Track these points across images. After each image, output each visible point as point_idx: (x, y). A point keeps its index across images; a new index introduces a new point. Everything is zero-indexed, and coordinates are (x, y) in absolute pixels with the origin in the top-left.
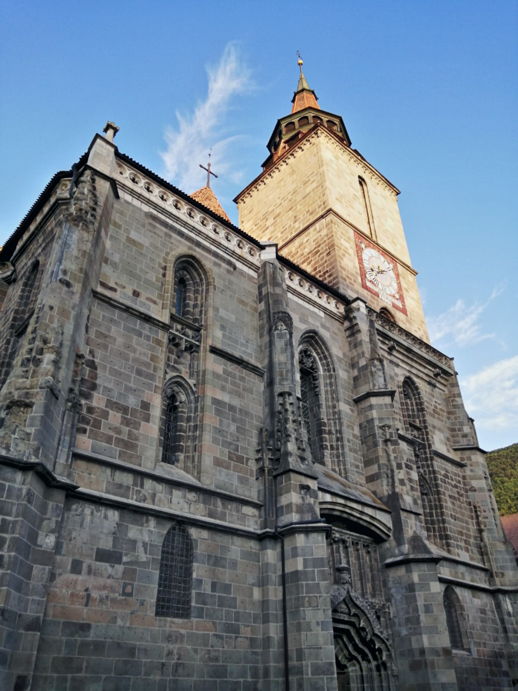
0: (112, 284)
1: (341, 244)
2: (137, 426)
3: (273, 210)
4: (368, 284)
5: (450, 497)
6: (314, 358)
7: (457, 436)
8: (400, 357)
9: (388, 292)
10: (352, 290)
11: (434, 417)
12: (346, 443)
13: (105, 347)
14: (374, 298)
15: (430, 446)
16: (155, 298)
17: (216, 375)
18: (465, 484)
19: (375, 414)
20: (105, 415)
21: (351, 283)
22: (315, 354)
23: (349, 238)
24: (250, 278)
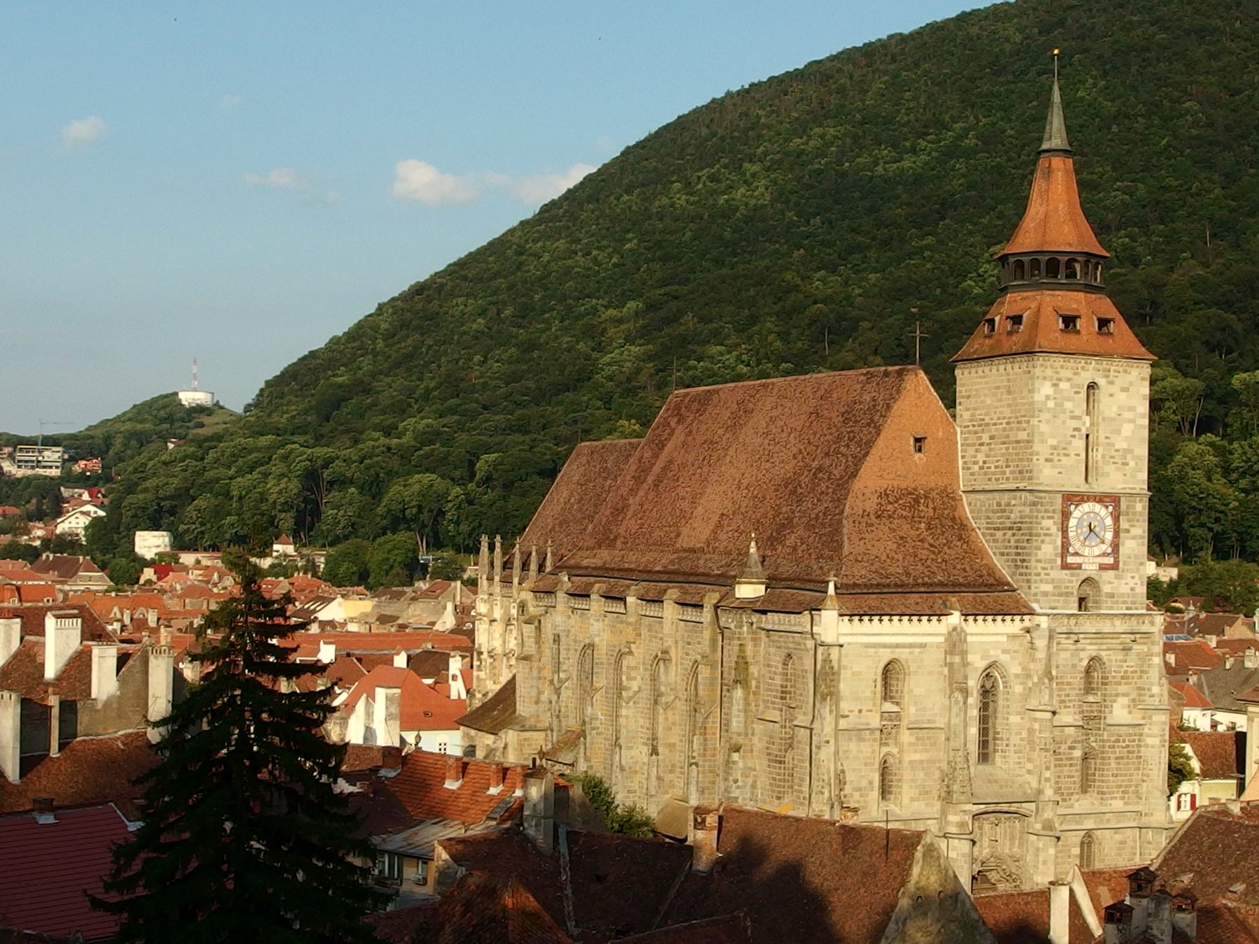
1: (1042, 529)
2: (867, 795)
3: (988, 424)
4: (1070, 560)
5: (1116, 758)
7: (1145, 695)
8: (1088, 641)
9: (1097, 551)
10: (1047, 583)
11: (1119, 684)
12: (1012, 748)
13: (848, 758)
14: (1072, 575)
15: (1105, 718)
16: (870, 708)
17: (911, 744)
18: (1139, 740)
19: (1036, 726)
20: (852, 795)
21: (1047, 574)
22: (996, 674)
23: (1054, 511)
24: (938, 645)
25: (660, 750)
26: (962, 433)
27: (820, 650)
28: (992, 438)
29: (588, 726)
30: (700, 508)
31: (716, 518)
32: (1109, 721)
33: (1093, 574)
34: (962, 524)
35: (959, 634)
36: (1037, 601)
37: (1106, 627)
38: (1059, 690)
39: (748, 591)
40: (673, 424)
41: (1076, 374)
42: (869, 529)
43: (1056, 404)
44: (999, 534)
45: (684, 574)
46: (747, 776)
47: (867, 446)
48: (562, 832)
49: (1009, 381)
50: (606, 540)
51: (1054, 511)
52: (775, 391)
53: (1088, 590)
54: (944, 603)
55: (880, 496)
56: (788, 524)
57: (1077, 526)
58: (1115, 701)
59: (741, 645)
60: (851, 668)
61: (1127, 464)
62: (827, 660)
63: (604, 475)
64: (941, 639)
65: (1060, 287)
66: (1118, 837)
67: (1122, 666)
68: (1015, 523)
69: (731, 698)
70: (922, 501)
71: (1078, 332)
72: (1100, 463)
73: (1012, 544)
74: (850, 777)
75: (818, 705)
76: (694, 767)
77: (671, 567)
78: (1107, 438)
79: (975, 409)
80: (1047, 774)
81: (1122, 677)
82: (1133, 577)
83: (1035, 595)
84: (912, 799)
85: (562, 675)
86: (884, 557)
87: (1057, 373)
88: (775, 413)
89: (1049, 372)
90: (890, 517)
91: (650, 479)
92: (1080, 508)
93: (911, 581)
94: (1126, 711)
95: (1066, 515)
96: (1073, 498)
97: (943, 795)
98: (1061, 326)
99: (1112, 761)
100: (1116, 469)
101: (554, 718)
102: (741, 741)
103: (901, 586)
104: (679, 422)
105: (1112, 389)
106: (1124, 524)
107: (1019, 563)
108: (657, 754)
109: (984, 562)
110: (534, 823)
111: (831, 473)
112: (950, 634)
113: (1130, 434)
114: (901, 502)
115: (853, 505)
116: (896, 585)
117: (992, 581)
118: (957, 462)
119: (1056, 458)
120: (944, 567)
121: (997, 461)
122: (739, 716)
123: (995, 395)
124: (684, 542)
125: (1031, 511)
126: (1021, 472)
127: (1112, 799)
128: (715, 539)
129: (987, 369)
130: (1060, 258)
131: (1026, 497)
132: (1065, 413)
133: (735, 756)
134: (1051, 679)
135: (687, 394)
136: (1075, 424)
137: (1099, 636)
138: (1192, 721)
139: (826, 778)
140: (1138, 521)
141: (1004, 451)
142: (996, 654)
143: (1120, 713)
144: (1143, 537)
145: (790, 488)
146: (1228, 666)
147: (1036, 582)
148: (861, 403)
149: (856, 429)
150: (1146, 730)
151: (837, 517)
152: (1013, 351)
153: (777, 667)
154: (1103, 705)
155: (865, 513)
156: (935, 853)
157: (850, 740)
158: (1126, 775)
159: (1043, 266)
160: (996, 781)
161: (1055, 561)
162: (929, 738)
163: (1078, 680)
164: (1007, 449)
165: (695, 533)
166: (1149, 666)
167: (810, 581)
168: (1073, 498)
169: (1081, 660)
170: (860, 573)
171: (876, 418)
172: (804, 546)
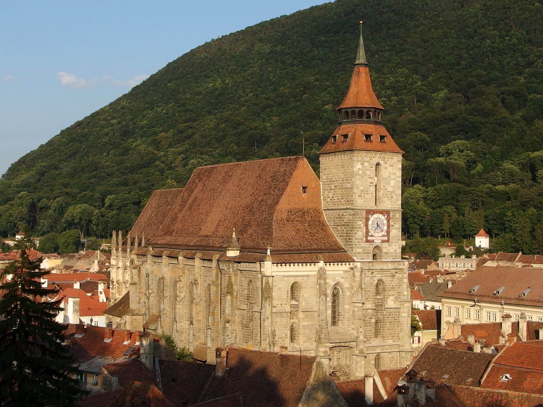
0: (276, 306)
1: (357, 225)
3: (334, 181)
4: (369, 238)
5: (389, 322)
6: (339, 289)
7: (401, 295)
8: (377, 273)
9: (380, 234)
10: (359, 248)
11: (390, 291)
14: (370, 245)
15: (384, 305)
16: (286, 303)
17: (303, 318)
18: (399, 314)
19: (356, 309)
22: (339, 287)
23: (362, 218)
24: (314, 276)
25: (194, 323)
26: (322, 185)
27: (264, 279)
28: (335, 187)
29: (162, 313)
30: (210, 218)
31: (216, 223)
32: (386, 307)
33: (379, 244)
34: (323, 224)
35: (323, 271)
36: (356, 256)
37: (385, 267)
38: (365, 294)
39: (232, 253)
40: (197, 182)
41: (371, 159)
42: (284, 226)
43: (363, 172)
44: (339, 228)
45: (203, 246)
46: (233, 333)
47: (283, 190)
48: (157, 360)
49: (343, 162)
50: (168, 232)
51: (362, 218)
52: (242, 167)
53: (377, 251)
54: (317, 258)
55: (288, 212)
56: (249, 225)
57: (372, 224)
58: (388, 298)
59: (229, 277)
60: (278, 286)
61: (392, 197)
62: (267, 283)
63: (166, 204)
64: (316, 273)
65: (364, 122)
66: (390, 356)
67: (391, 283)
68: (346, 223)
69: (225, 300)
70: (306, 214)
71: (372, 141)
72: (381, 197)
73: (345, 232)
74: (277, 333)
75: (263, 302)
76: (209, 330)
77: (197, 243)
78: (384, 186)
79: (328, 174)
80: (361, 330)
81: (391, 288)
82: (395, 245)
83: (355, 253)
84: (304, 342)
85: (150, 291)
86: (290, 238)
87: (363, 159)
88: (241, 177)
89: (360, 158)
90: (292, 221)
91: (187, 206)
92: (373, 216)
93: (302, 248)
94: (393, 302)
95: (367, 219)
96: (370, 212)
97: (317, 339)
98: (365, 139)
99: (388, 324)
100: (388, 200)
101: (147, 310)
102: (230, 319)
103: (298, 250)
104: (199, 181)
105: (386, 166)
106: (391, 223)
107: (348, 240)
108: (193, 325)
109: (333, 239)
110: (144, 357)
111: (267, 202)
112: (319, 271)
113: (394, 185)
114: (297, 214)
115: (277, 216)
116: (296, 250)
117: (336, 248)
118: (321, 197)
119: (363, 195)
120: (316, 242)
121: (338, 197)
122: (229, 308)
123: (337, 168)
124: (203, 233)
125: (353, 218)
126: (348, 201)
127: (387, 339)
128: (217, 231)
129: (333, 157)
130: (364, 110)
131: (350, 212)
132: (367, 176)
133: (228, 325)
134: (362, 289)
135: (202, 169)
136: (371, 180)
137: (382, 270)
138: (416, 305)
139: (267, 333)
140: (397, 221)
141: (341, 192)
142: (338, 279)
143: (390, 303)
144: (400, 228)
145: (249, 209)
146: (430, 282)
147: (355, 248)
148: (279, 172)
149: (277, 183)
150: (402, 310)
151: (270, 221)
152: (345, 150)
153: (245, 286)
154: (384, 300)
155: (282, 220)
156: (321, 366)
157: (277, 317)
158: (393, 329)
159: (357, 113)
160: (339, 333)
161: (363, 239)
162: (311, 315)
163: (373, 289)
164: (342, 191)
165: (208, 229)
166: (403, 283)
167: (260, 249)
168: (370, 212)
169: (374, 281)
170: (280, 245)
171: (286, 178)
172: (256, 234)
